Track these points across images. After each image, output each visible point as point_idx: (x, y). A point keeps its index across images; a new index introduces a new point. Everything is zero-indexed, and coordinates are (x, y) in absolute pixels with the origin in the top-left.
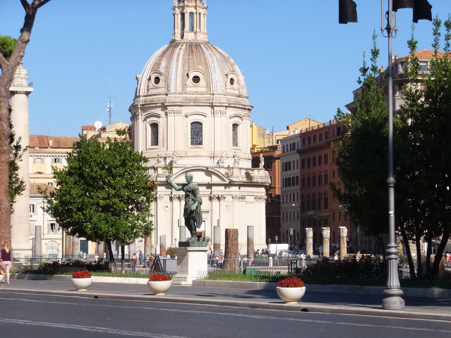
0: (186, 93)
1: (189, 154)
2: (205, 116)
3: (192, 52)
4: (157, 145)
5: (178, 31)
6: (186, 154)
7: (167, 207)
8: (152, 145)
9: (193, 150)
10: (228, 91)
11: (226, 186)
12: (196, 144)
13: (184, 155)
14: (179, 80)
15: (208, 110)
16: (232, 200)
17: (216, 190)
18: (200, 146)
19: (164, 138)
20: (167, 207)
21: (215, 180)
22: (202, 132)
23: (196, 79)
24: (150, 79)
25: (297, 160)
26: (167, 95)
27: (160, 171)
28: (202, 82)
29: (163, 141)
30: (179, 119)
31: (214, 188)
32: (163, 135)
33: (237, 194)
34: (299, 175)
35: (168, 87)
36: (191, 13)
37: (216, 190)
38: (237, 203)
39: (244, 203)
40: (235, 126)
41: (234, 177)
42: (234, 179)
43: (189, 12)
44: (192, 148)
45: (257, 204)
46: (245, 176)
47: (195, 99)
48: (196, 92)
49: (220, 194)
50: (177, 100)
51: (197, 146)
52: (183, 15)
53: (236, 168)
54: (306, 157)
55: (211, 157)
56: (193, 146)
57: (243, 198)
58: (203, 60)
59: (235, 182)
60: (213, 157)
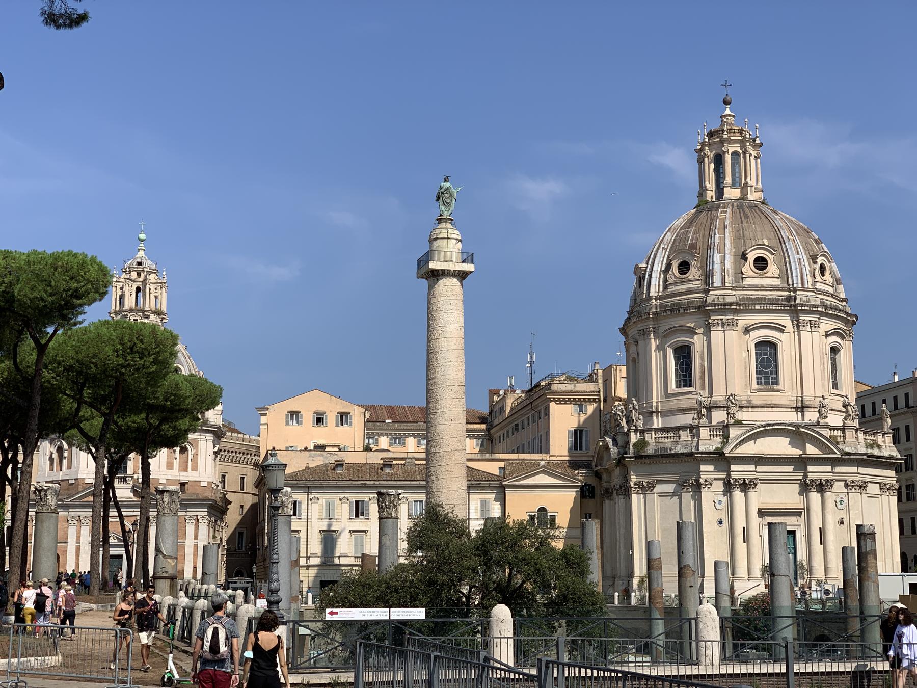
0: (744, 289)
1: (755, 402)
2: (782, 331)
3: (747, 217)
4: (691, 386)
5: (711, 185)
7: (720, 502)
8: (678, 386)
10: (818, 286)
11: (835, 462)
13: (744, 403)
14: (728, 265)
15: (785, 320)
17: (816, 472)
18: (775, 387)
19: (703, 372)
20: (720, 502)
21: (812, 450)
22: (776, 360)
23: (761, 263)
24: (669, 266)
25: (907, 427)
26: (706, 292)
27: (704, 433)
28: (772, 268)
29: (702, 378)
30: (733, 336)
32: (702, 366)
33: (855, 477)
35: (708, 276)
36: (735, 153)
37: (816, 472)
38: (855, 496)
40: (834, 350)
42: (847, 450)
43: (731, 151)
44: (759, 390)
45: (885, 498)
49: (824, 477)
50: (729, 300)
52: (719, 160)
55: (796, 408)
56: (760, 387)
59: (850, 454)
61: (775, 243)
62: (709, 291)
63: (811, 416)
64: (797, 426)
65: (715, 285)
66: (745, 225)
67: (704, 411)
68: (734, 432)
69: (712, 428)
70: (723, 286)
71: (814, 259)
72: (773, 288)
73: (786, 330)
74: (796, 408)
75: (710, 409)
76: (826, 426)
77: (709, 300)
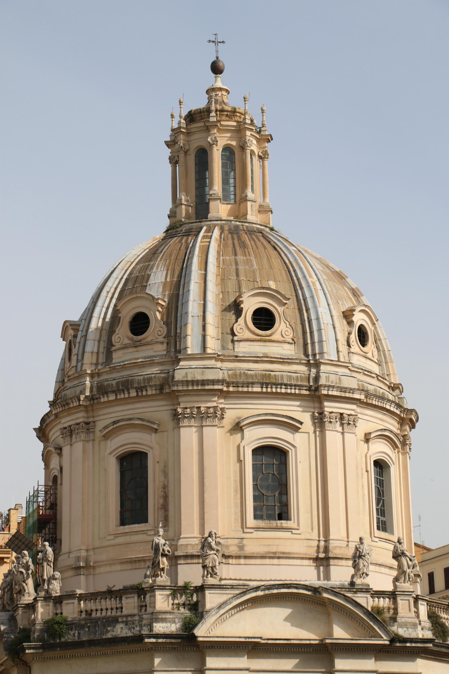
0: (237, 359)
1: (250, 549)
6: (241, 548)
12: (270, 517)
13: (233, 550)
28: (282, 328)
30: (216, 435)
47: (264, 376)
50: (210, 375)
53: (405, 593)
59: (405, 640)
60: (327, 559)
61: (286, 289)
62: (180, 360)
63: (341, 574)
64: (315, 590)
65: (189, 352)
66: (240, 258)
67: (164, 562)
68: (212, 599)
69: (177, 590)
70: (203, 355)
71: (348, 316)
72: (283, 361)
73: (303, 428)
74: (316, 559)
75: (174, 560)
76: (367, 590)
77: (179, 375)
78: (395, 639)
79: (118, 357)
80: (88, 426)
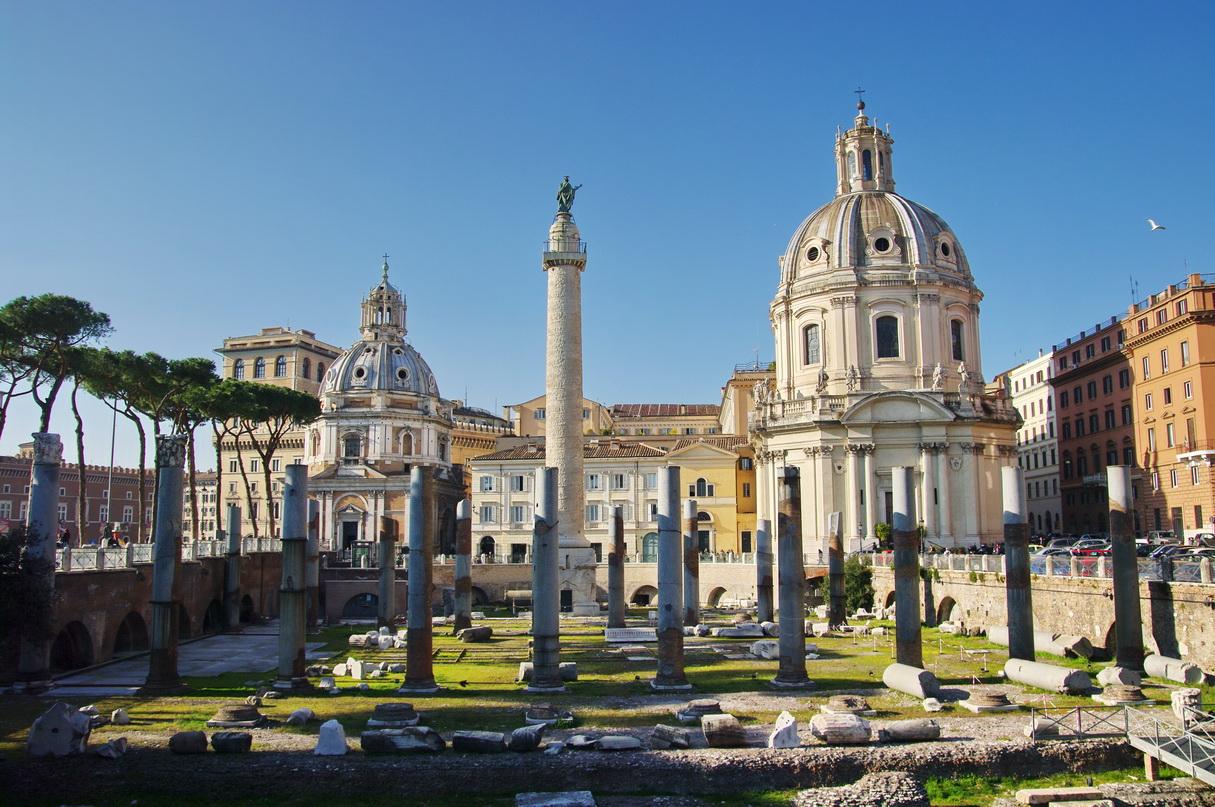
3: (873, 204)
9: (883, 366)
10: (940, 263)
11: (948, 425)
15: (905, 294)
16: (960, 451)
21: (924, 413)
31: (926, 431)
34: (1054, 421)
38: (969, 458)
39: (979, 457)
40: (956, 325)
41: (962, 411)
42: (962, 414)
44: (880, 363)
46: (981, 409)
48: (884, 266)
51: (889, 359)
54: (1070, 388)
56: (881, 359)
57: (979, 449)
58: (891, 215)
78: (958, 417)
79: (802, 273)
80: (788, 313)
